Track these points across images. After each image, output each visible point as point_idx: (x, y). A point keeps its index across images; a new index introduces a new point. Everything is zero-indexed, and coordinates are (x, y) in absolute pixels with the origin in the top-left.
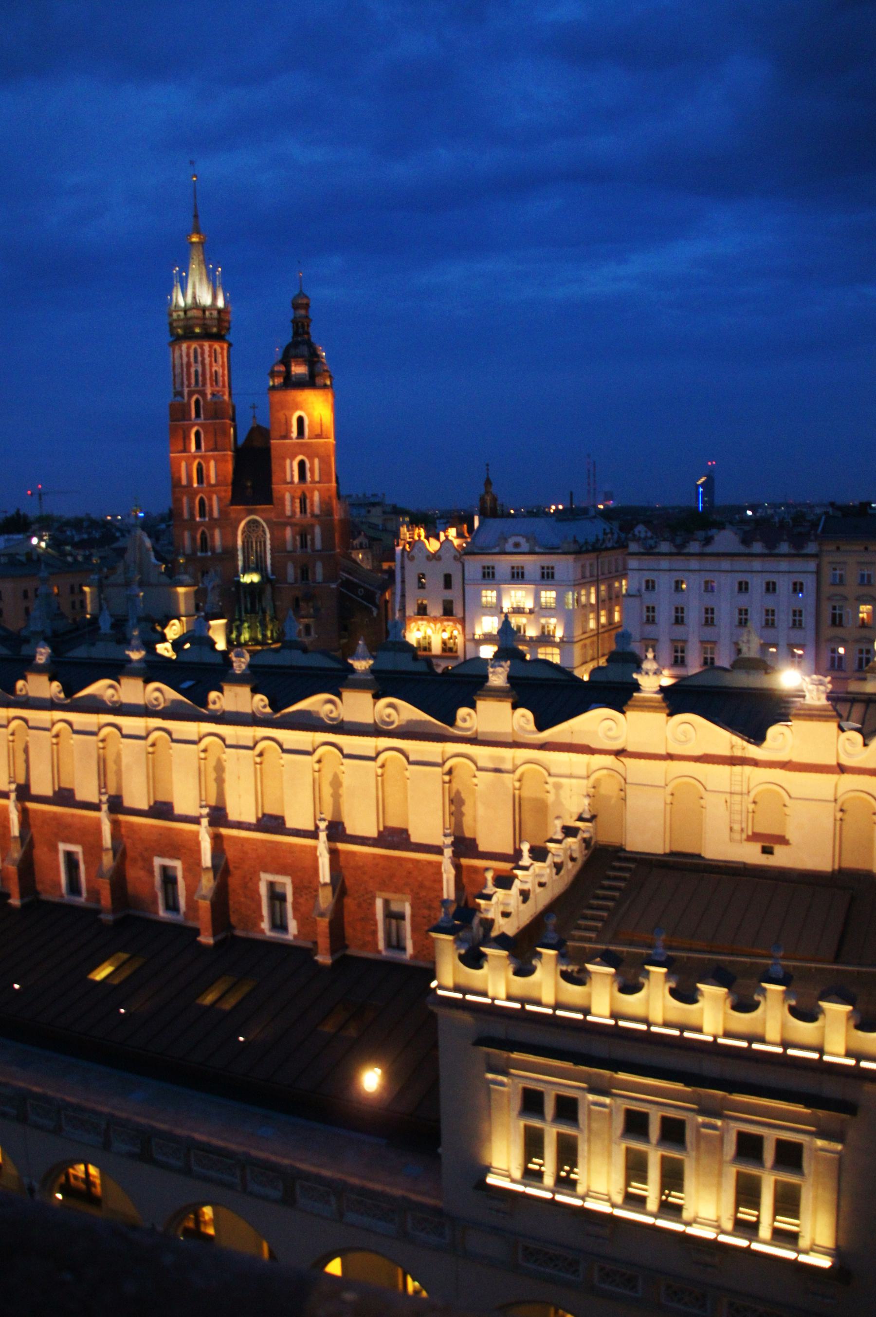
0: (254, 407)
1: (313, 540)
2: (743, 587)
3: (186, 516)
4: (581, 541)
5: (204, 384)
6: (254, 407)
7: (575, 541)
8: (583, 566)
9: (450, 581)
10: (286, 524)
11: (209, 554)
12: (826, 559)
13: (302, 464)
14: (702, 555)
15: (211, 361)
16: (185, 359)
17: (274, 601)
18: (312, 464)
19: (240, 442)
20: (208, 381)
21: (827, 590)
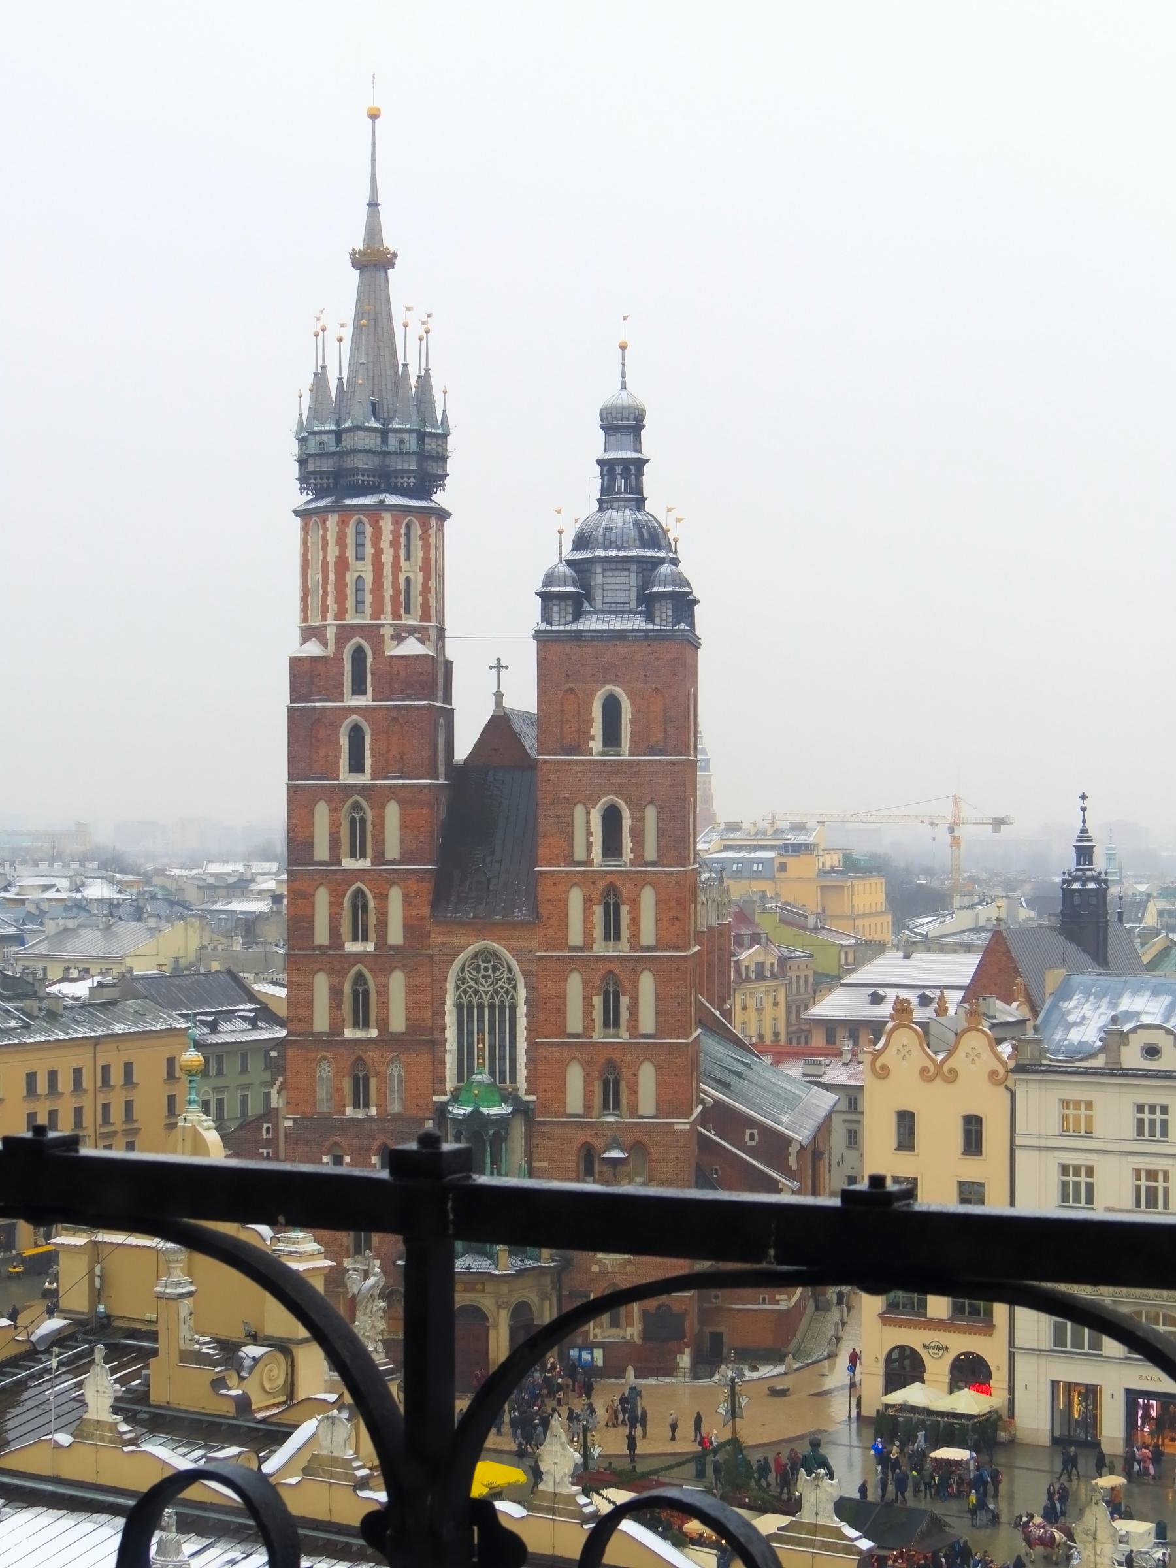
1: (634, 1007)
3: (322, 936)
5: (377, 613)
6: (499, 667)
9: (979, 1134)
10: (565, 966)
11: (374, 1033)
13: (612, 818)
15: (396, 557)
16: (333, 552)
18: (638, 820)
19: (463, 749)
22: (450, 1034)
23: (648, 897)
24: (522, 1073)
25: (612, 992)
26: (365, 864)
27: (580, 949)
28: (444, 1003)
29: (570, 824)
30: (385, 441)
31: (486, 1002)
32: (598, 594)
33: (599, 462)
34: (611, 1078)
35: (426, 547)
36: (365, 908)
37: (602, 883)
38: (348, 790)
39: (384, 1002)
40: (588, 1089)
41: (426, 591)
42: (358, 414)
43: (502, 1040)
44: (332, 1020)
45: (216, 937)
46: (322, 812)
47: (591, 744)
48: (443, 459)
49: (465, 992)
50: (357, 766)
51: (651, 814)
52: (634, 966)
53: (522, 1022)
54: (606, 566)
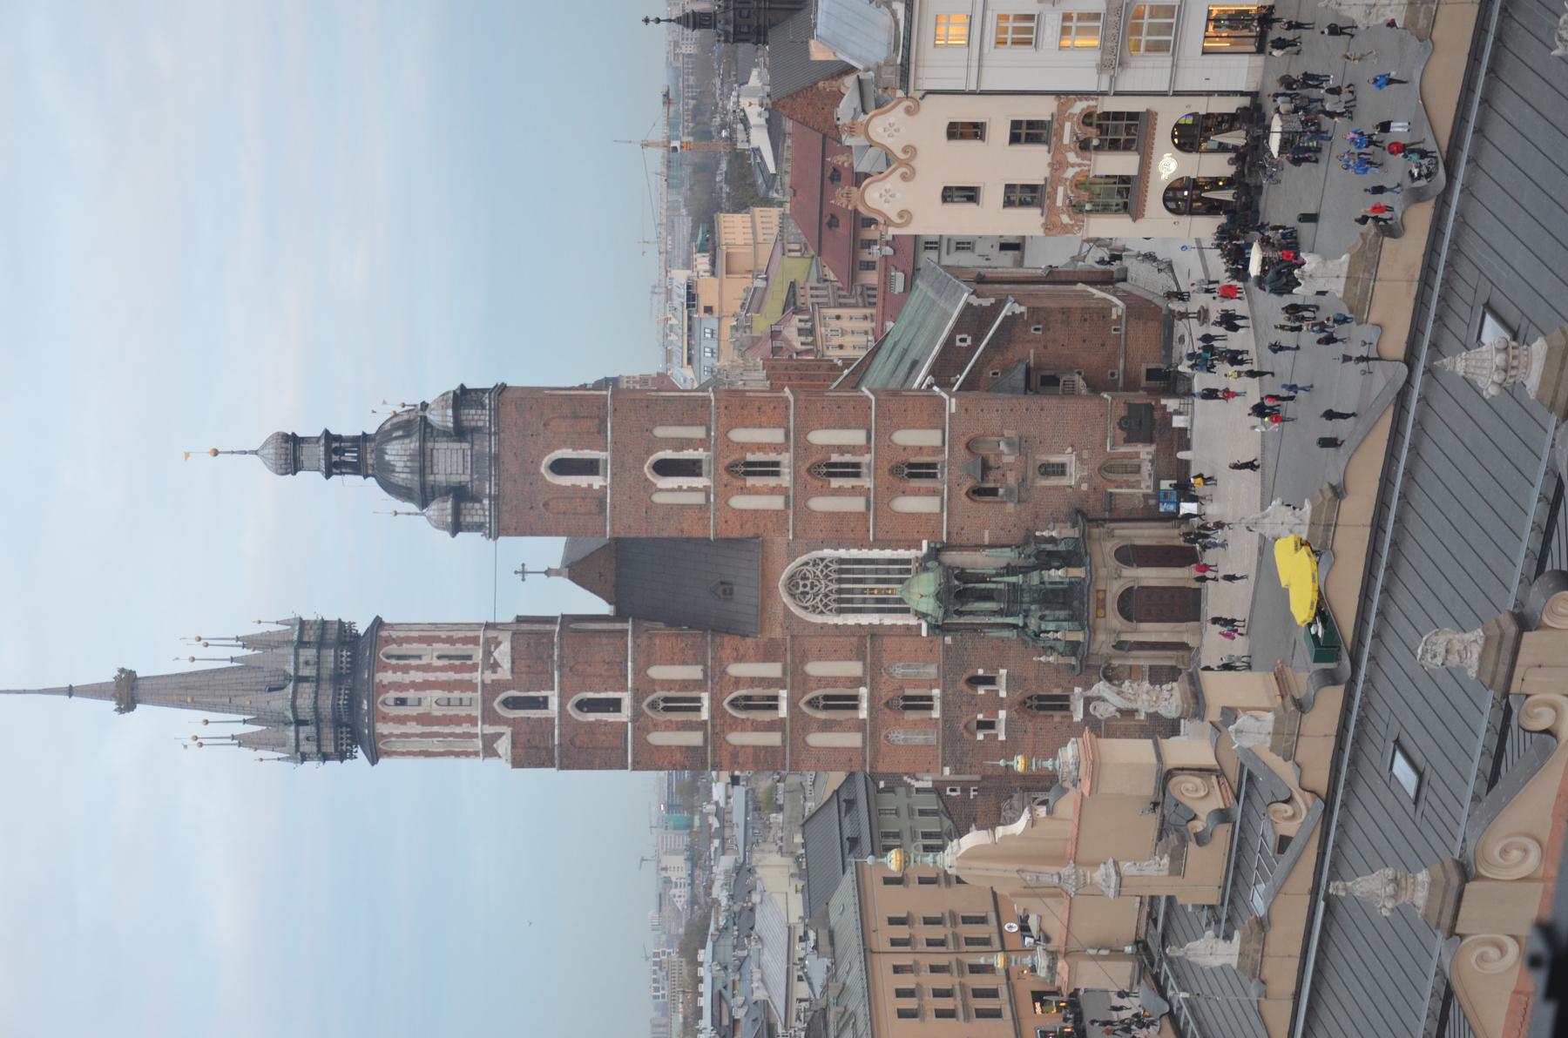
0: (523, 573)
1: (841, 449)
3: (774, 739)
5: (470, 686)
9: (964, 125)
17: (978, 547)
19: (602, 607)
20: (466, 676)
23: (739, 435)
26: (705, 697)
27: (787, 497)
28: (836, 626)
29: (671, 507)
30: (306, 679)
31: (835, 586)
32: (455, 479)
33: (328, 475)
34: (907, 471)
35: (409, 640)
36: (748, 698)
37: (726, 478)
38: (637, 715)
39: (834, 681)
40: (917, 493)
41: (451, 641)
42: (279, 702)
43: (871, 571)
44: (849, 729)
45: (770, 839)
46: (657, 738)
47: (596, 486)
48: (324, 624)
49: (826, 606)
50: (615, 705)
52: (803, 448)
53: (854, 553)
54: (428, 471)
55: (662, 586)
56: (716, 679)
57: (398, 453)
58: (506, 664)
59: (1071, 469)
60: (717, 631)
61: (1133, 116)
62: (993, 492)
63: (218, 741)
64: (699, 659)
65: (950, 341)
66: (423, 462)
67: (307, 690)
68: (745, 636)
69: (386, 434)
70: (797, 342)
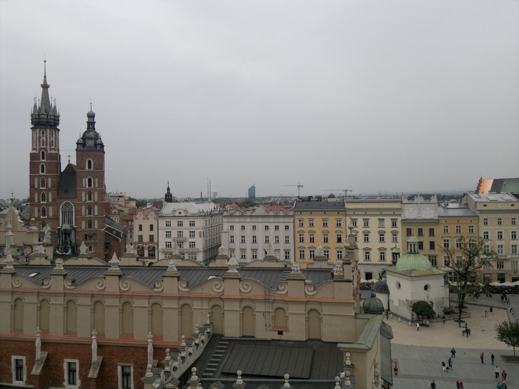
1: (94, 211)
2: (267, 228)
3: (36, 201)
4: (205, 211)
5: (47, 145)
7: (203, 212)
8: (206, 221)
10: (81, 205)
12: (297, 218)
13: (90, 180)
14: (251, 216)
16: (38, 135)
17: (75, 236)
19: (63, 170)
20: (48, 145)
21: (298, 229)
22: (61, 217)
23: (96, 193)
24: (74, 223)
25: (90, 209)
26: (45, 188)
35: (56, 135)
38: (41, 176)
39: (48, 211)
40: (86, 225)
41: (56, 142)
42: (43, 112)
46: (36, 180)
48: (59, 121)
50: (43, 172)
51: (97, 179)
52: (94, 204)
53: (74, 214)
55: (68, 181)
56: (48, 190)
57: (92, 134)
58: (51, 152)
59: (91, 252)
60: (58, 190)
61: (154, 255)
62: (86, 238)
63: (35, 101)
64: (52, 187)
65: (114, 230)
66: (90, 138)
67: (46, 117)
68: (57, 195)
69: (95, 132)
70: (113, 212)
